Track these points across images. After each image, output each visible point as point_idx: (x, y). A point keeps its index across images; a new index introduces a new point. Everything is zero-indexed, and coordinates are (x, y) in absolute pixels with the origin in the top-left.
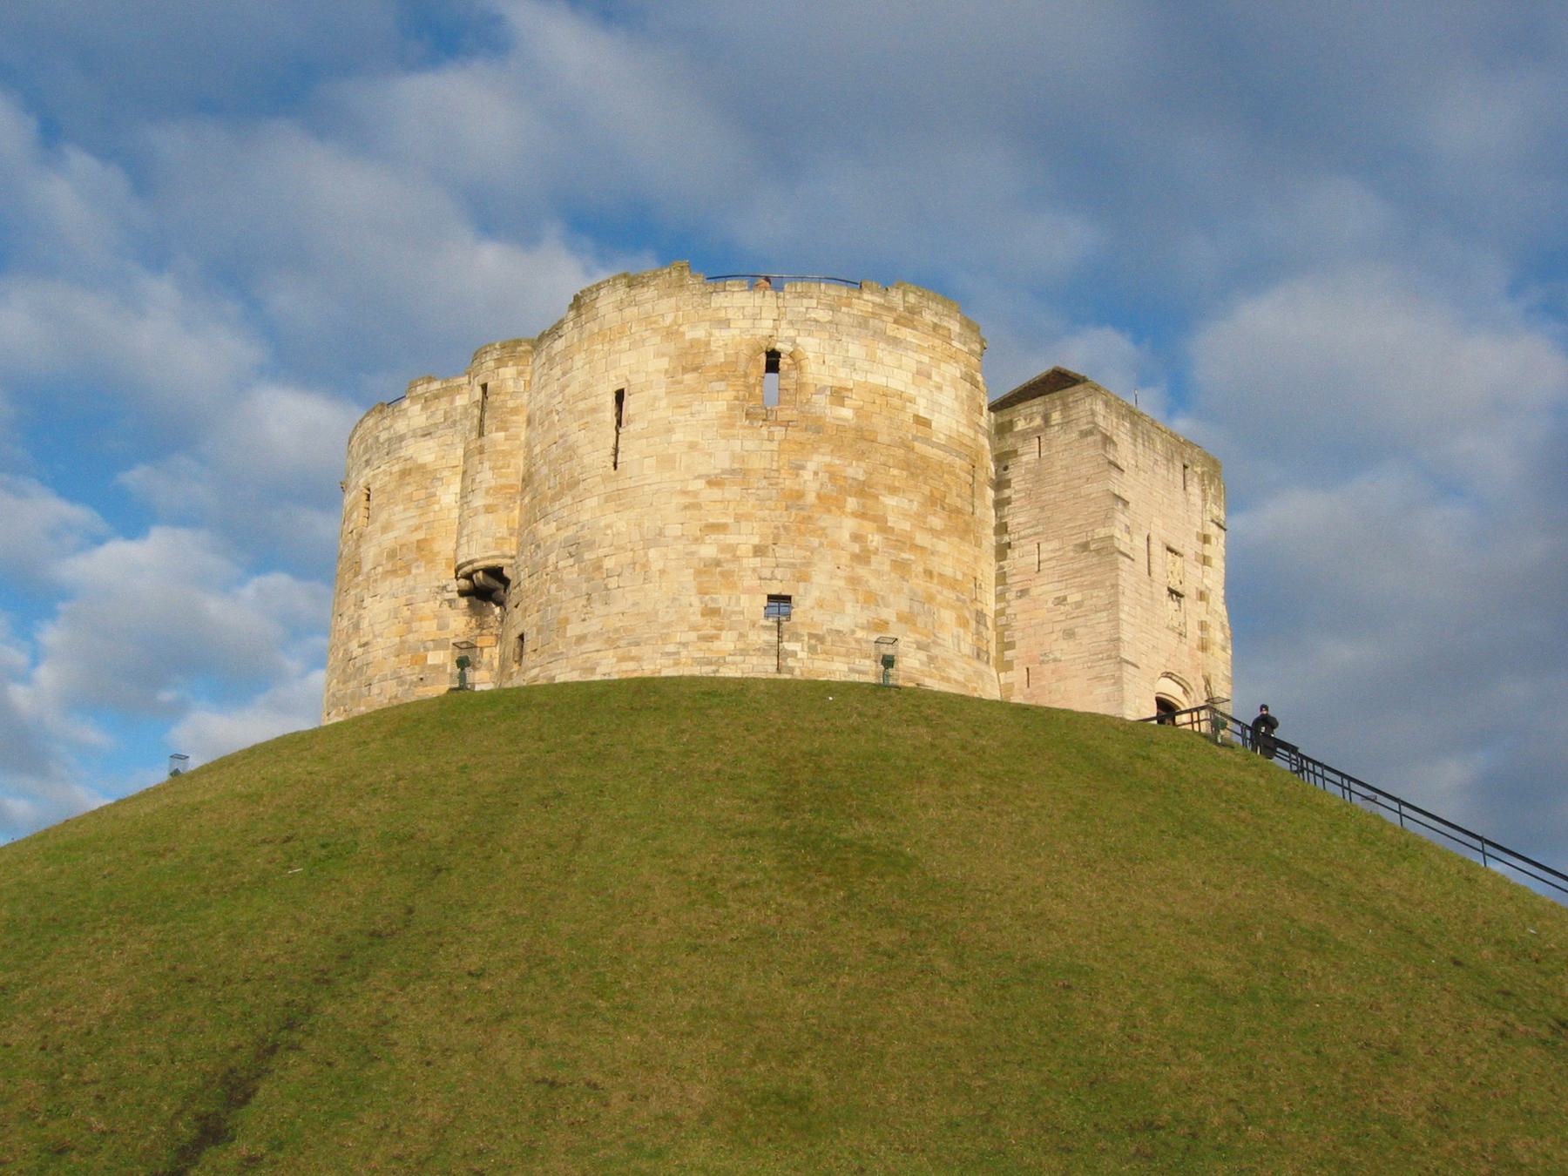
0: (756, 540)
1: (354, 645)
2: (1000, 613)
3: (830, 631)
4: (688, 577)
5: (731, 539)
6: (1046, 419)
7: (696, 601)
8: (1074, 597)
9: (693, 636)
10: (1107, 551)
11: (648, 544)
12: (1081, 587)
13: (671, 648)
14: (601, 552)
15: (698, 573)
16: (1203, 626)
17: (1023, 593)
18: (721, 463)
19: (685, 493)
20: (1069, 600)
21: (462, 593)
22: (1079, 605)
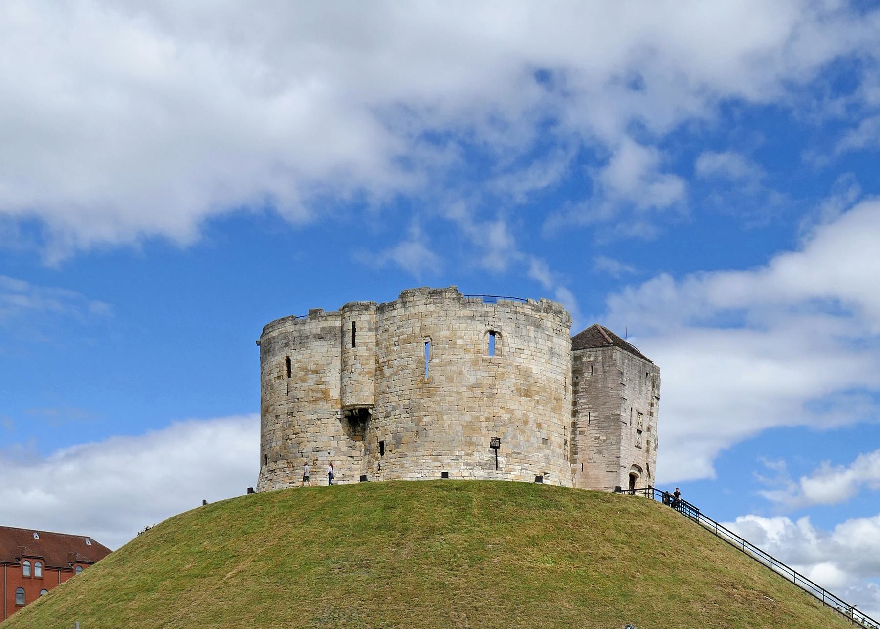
0: (486, 414)
2: (573, 439)
3: (514, 453)
4: (460, 428)
6: (596, 358)
9: (463, 453)
10: (617, 419)
12: (606, 434)
13: (454, 458)
15: (464, 427)
16: (648, 442)
17: (582, 433)
18: (472, 380)
20: (602, 438)
21: (346, 417)
22: (605, 441)
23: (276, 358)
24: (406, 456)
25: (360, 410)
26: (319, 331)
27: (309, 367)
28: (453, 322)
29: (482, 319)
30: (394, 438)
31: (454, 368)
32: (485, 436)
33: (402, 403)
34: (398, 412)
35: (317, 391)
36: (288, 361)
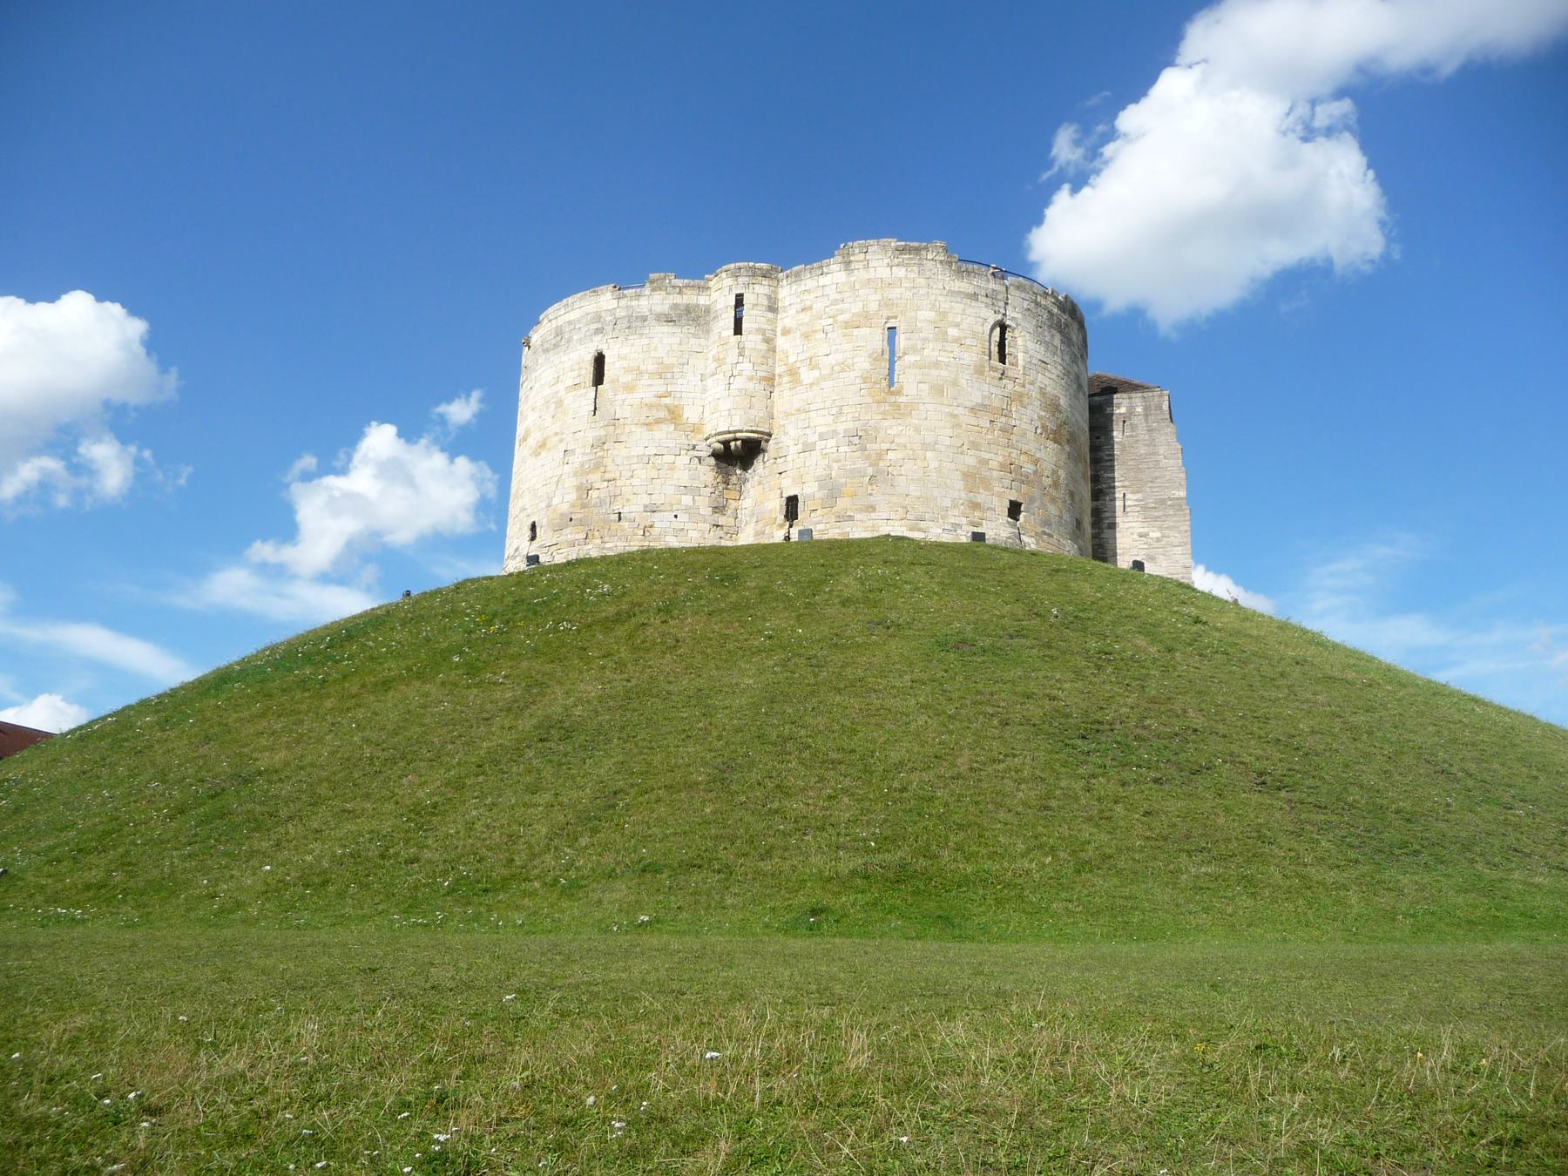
0: (1000, 459)
1: (595, 478)
5: (987, 456)
7: (963, 495)
8: (1152, 535)
11: (926, 447)
12: (1160, 528)
14: (885, 446)
15: (966, 476)
18: (976, 398)
19: (955, 416)
20: (1152, 535)
21: (715, 455)
22: (1158, 540)
23: (574, 355)
24: (851, 518)
25: (745, 441)
26: (666, 309)
27: (643, 368)
28: (941, 298)
29: (989, 301)
30: (821, 487)
31: (944, 373)
32: (1000, 495)
33: (841, 428)
34: (832, 443)
35: (657, 406)
36: (600, 360)
